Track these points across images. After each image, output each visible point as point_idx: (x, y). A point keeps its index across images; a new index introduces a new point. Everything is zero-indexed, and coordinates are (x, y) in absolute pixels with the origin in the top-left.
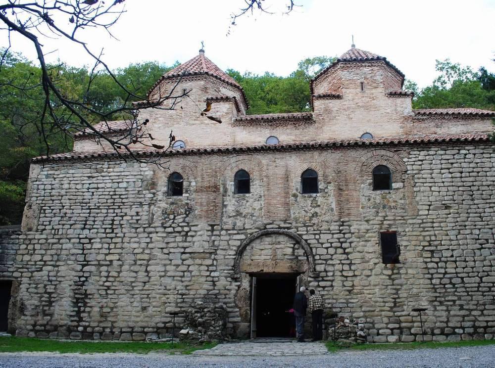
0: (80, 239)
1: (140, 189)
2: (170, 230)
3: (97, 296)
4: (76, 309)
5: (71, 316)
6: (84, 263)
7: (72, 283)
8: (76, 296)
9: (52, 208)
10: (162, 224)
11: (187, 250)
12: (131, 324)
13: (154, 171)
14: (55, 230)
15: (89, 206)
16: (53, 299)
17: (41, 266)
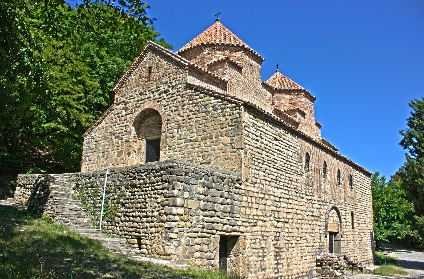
0: (275, 196)
1: (297, 160)
2: (308, 197)
3: (285, 249)
4: (276, 262)
5: (275, 268)
6: (278, 219)
7: (273, 238)
8: (277, 250)
9: (259, 161)
10: (305, 192)
11: (314, 215)
12: (298, 271)
13: (301, 148)
14: (262, 184)
15: (278, 167)
16: (265, 254)
17: (257, 221)
